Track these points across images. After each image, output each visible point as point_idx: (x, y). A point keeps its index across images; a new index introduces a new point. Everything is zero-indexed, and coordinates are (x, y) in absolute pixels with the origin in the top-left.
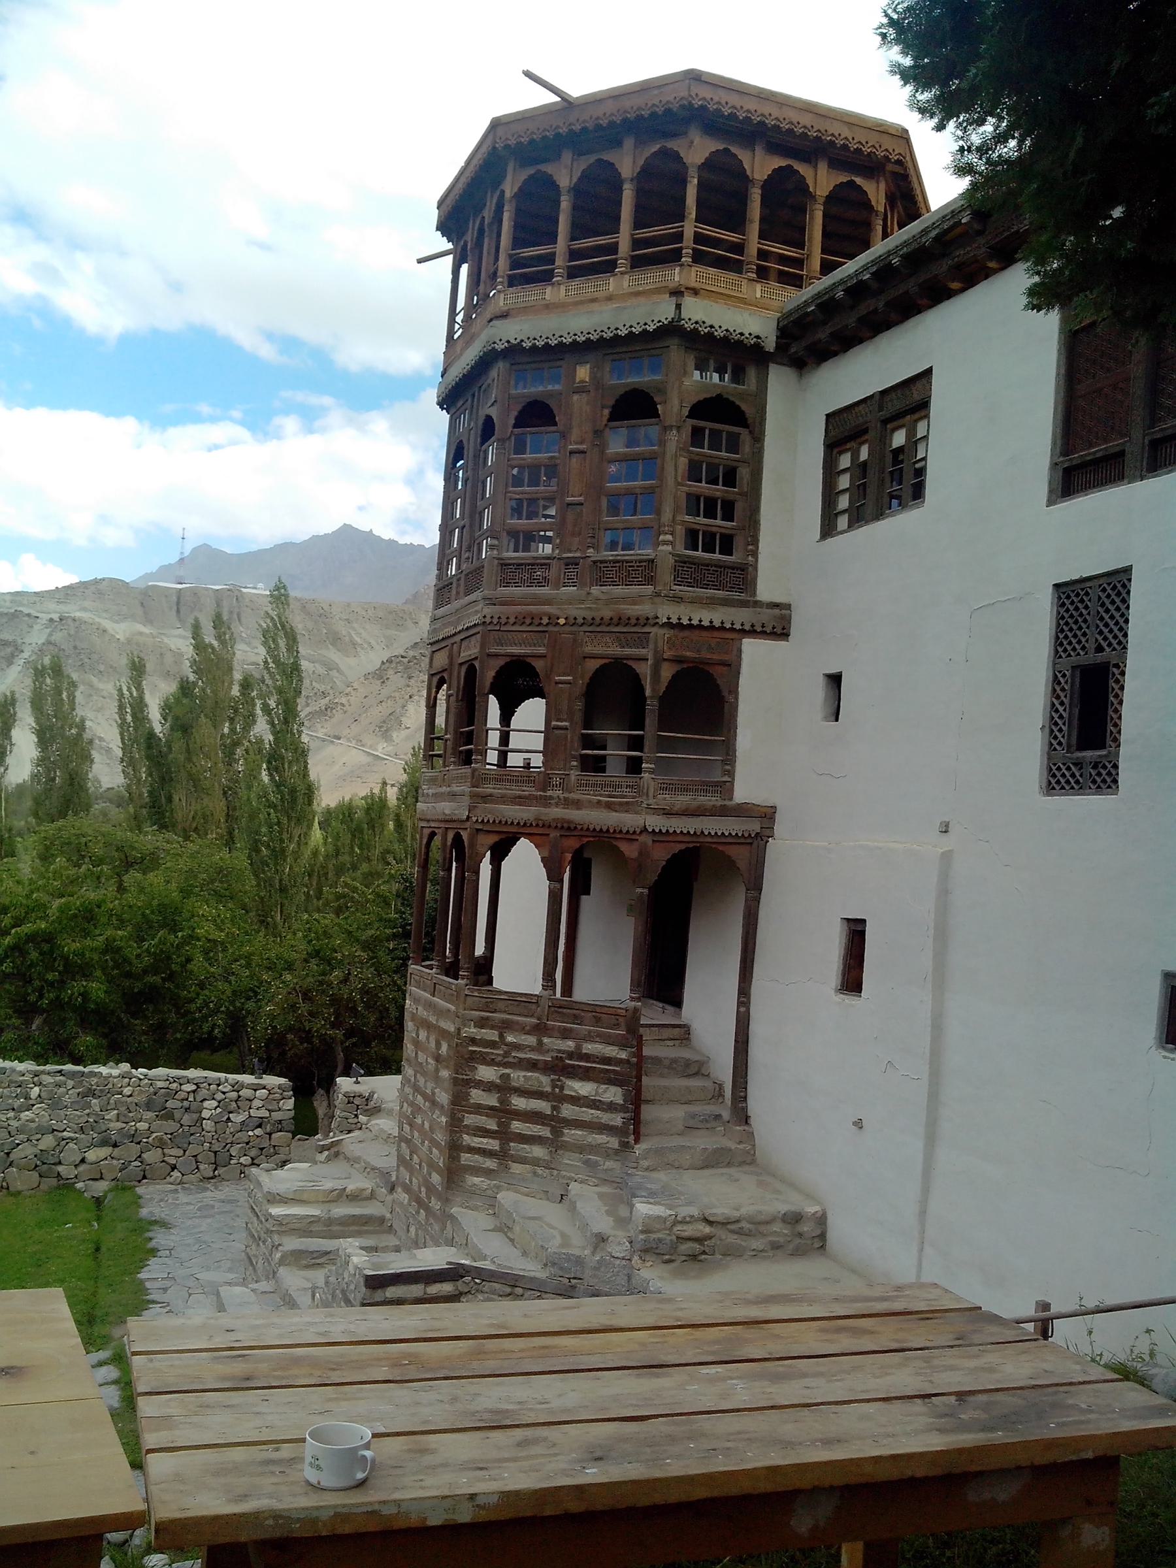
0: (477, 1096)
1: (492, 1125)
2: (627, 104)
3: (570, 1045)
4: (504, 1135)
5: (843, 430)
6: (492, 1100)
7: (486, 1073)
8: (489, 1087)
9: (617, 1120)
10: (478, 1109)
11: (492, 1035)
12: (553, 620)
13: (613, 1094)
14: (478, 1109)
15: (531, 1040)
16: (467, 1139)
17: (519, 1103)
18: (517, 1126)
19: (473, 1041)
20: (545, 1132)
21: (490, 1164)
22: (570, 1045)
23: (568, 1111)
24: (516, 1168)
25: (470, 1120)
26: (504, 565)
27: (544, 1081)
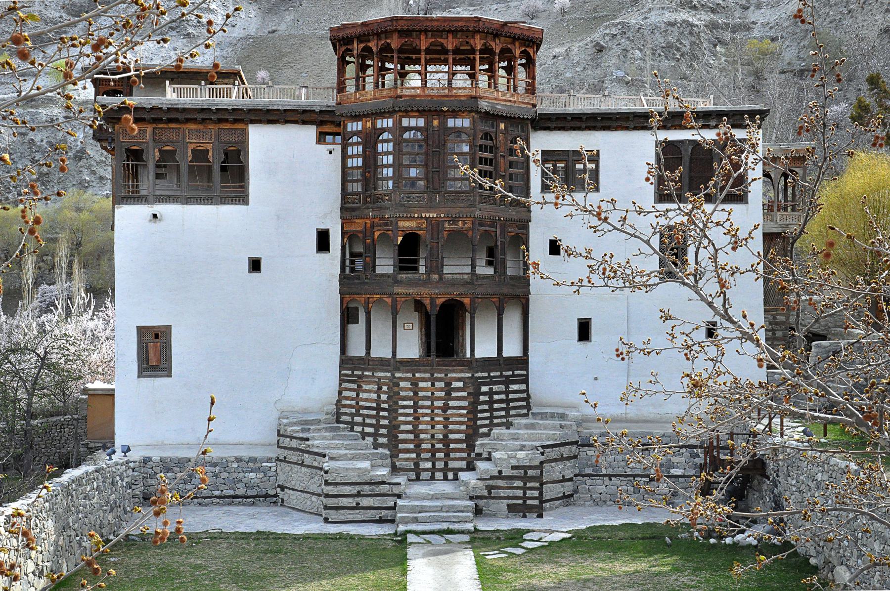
0: (483, 398)
1: (487, 407)
2: (525, 33)
3: (510, 373)
4: (491, 410)
5: (548, 156)
6: (486, 398)
7: (484, 389)
8: (485, 394)
9: (525, 395)
10: (484, 403)
11: (486, 374)
12: (499, 219)
13: (523, 387)
14: (484, 403)
15: (498, 374)
16: (479, 415)
17: (496, 397)
18: (495, 406)
19: (480, 378)
20: (504, 405)
21: (487, 422)
22: (510, 373)
23: (511, 396)
24: (495, 421)
25: (480, 408)
26: (481, 196)
27: (502, 388)
